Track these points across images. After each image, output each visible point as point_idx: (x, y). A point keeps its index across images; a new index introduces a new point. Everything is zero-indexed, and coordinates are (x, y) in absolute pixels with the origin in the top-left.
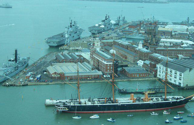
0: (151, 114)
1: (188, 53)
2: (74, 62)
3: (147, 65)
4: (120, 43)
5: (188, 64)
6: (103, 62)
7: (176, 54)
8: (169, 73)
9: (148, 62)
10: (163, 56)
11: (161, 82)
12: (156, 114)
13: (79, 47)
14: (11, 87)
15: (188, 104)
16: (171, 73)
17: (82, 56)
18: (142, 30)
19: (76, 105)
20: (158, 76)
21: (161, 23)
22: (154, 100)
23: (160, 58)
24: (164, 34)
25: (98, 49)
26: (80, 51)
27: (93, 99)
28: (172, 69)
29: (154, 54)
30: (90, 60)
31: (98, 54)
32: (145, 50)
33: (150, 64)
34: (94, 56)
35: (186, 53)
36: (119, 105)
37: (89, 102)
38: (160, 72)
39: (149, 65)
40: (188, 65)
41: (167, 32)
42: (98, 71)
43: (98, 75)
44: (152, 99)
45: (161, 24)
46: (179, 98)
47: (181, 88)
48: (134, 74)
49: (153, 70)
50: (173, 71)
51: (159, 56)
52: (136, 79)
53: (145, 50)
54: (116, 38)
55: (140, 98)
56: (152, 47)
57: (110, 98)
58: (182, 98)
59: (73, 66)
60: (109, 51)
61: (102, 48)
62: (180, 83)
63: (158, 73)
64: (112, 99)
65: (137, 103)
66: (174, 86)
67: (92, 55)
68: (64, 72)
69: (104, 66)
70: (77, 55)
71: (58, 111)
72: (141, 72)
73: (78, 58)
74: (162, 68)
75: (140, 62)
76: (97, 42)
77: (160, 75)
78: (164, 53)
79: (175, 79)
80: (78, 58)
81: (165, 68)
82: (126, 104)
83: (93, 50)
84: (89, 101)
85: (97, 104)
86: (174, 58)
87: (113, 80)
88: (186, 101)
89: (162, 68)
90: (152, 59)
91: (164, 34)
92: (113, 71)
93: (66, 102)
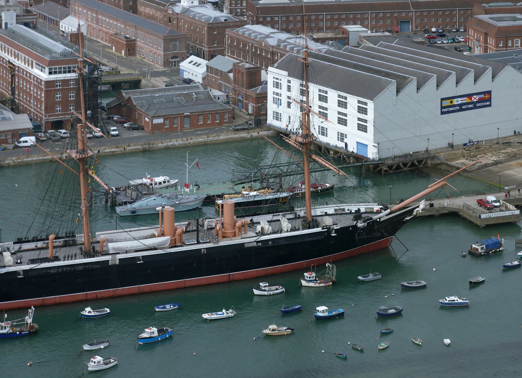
0: (256, 292)
1: (384, 18)
3: (223, 75)
6: (36, 71)
7: (336, 24)
8: (315, 104)
10: (284, 36)
11: (288, 146)
15: (401, 235)
16: (324, 104)
20: (271, 120)
22: (259, 228)
23: (272, 42)
29: (247, 26)
33: (235, 69)
36: (114, 266)
38: (278, 102)
39: (231, 75)
40: (391, 68)
42: (9, 114)
46: (363, 210)
49: (247, 97)
50: (333, 95)
52: (177, 137)
55: (203, 226)
60: (57, 24)
63: (271, 107)
64: (81, 238)
69: (38, 88)
72: (200, 108)
75: (191, 66)
77: (277, 116)
78: (288, 22)
79: (342, 129)
81: (296, 84)
82: (143, 257)
87: (84, 151)
92: (78, 108)
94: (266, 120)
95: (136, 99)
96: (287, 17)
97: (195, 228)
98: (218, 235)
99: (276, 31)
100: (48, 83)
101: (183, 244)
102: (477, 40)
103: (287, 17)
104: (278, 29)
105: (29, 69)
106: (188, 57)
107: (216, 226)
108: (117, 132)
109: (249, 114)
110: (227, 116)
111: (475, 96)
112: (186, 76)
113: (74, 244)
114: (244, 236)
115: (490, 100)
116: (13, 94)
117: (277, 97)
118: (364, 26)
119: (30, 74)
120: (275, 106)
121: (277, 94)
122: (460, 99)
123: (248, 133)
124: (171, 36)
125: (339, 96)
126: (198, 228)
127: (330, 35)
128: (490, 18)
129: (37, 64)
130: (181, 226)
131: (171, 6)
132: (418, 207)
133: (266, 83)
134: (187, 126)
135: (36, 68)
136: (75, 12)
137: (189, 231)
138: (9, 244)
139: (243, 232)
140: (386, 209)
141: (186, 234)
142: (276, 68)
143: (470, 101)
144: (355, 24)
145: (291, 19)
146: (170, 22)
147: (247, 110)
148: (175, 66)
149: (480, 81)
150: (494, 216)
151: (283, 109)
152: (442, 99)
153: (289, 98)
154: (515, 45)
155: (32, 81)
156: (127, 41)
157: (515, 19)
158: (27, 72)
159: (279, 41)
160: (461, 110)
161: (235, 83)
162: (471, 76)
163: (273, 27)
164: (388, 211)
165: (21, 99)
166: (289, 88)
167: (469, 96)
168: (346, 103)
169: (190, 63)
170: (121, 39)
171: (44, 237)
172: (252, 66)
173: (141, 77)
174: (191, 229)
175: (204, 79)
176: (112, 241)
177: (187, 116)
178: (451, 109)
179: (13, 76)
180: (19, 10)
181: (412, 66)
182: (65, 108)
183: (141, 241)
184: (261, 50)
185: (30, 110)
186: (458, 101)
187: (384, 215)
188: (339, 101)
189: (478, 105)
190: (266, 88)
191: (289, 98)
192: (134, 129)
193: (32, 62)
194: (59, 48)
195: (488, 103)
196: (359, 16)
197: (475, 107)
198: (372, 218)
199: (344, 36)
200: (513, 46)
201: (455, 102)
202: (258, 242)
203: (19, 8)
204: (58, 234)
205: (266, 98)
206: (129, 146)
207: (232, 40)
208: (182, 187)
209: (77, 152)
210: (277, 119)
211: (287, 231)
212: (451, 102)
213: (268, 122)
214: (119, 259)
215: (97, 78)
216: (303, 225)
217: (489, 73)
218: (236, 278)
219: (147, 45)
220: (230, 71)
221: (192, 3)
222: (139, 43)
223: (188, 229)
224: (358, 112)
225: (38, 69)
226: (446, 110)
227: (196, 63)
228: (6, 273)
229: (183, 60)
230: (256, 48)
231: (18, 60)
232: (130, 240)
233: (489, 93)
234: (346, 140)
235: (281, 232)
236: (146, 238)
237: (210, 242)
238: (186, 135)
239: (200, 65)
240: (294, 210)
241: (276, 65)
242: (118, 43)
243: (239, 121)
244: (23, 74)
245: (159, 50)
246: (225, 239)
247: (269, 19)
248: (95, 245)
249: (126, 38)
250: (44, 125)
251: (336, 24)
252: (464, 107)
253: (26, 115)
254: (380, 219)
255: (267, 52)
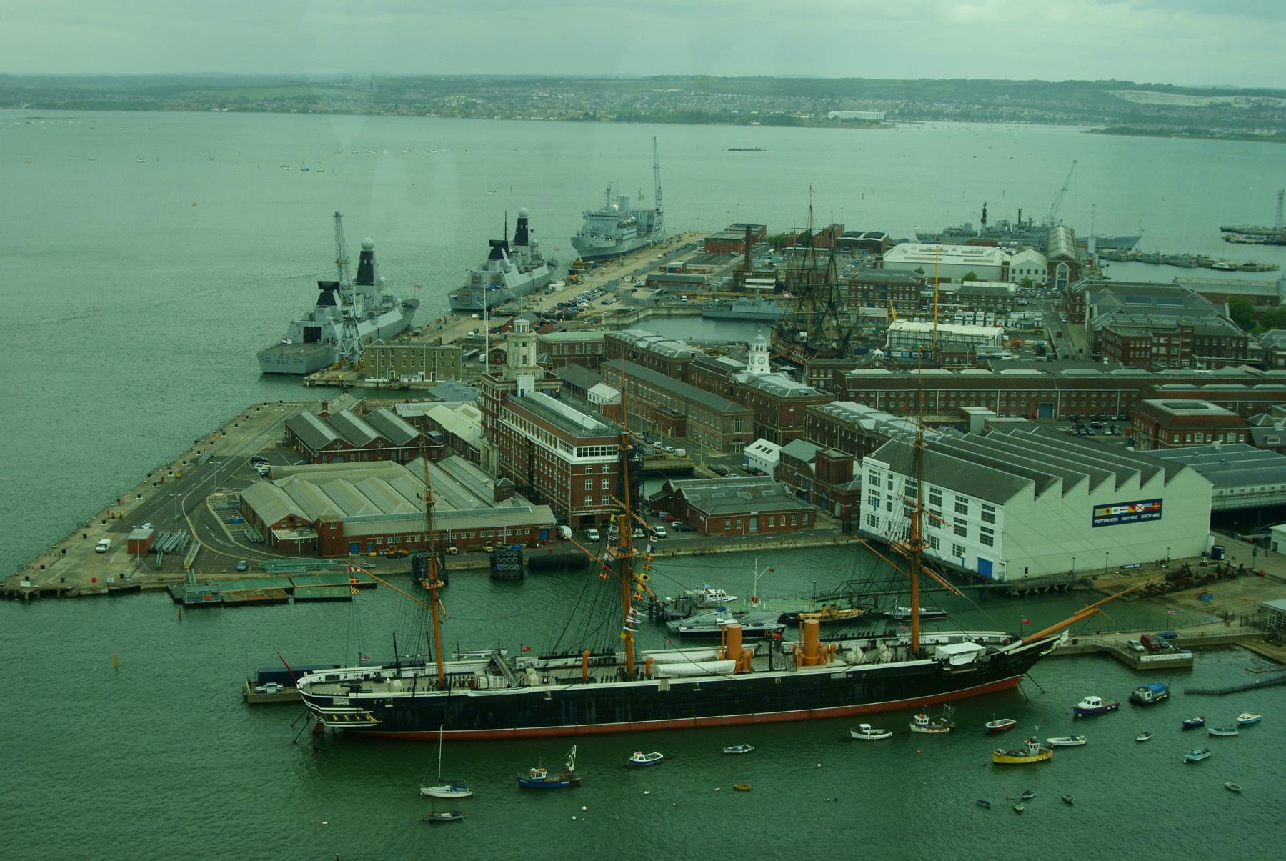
2: (393, 455)
3: (803, 466)
4: (642, 345)
5: (1026, 454)
6: (560, 452)
9: (804, 450)
10: (884, 417)
12: (882, 735)
13: (413, 372)
14: (47, 609)
15: (1033, 671)
17: (435, 425)
18: (757, 275)
19: (420, 694)
20: (864, 526)
21: (857, 234)
22: (851, 656)
23: (868, 424)
24: (884, 295)
25: (527, 384)
26: (423, 394)
27: (513, 660)
28: (939, 488)
29: (837, 403)
30: (481, 444)
31: (531, 410)
32: (783, 383)
33: (819, 458)
34: (506, 422)
35: (1008, 398)
36: (664, 692)
37: (491, 677)
38: (875, 503)
39: (813, 466)
41: (898, 285)
42: (525, 504)
43: (534, 528)
44: (841, 651)
45: (861, 238)
47: (992, 590)
48: (733, 518)
49: (835, 495)
51: (864, 417)
52: (741, 542)
53: (783, 383)
54: (614, 321)
56: (819, 368)
57: (610, 652)
58: (1005, 644)
59: (388, 479)
61: (548, 376)
62: (985, 565)
63: (866, 509)
64: (620, 656)
65: (760, 673)
66: (957, 575)
67: (494, 416)
68: (343, 516)
69: (563, 473)
70: (406, 419)
71: (318, 731)
72: (772, 507)
73: (413, 432)
74: (884, 478)
75: (759, 453)
76: (520, 342)
77: (873, 521)
78: (888, 398)
79: (959, 540)
80: (413, 432)
81: (900, 481)
83: (500, 388)
84: (493, 667)
85: (535, 685)
86: (947, 424)
88: (1028, 659)
89: (884, 478)
90: (826, 431)
91: (884, 295)
93: (367, 677)
94: (858, 525)
95: (688, 492)
96: (888, 394)
97: (767, 652)
98: (795, 661)
99: (874, 410)
100: (578, 468)
101: (753, 671)
102: (1144, 432)
103: (888, 394)
104: (875, 407)
105: (552, 449)
106: (755, 440)
107: (794, 650)
108: (664, 533)
109: (835, 517)
110: (806, 518)
111: (1140, 505)
112: (752, 464)
113: (614, 664)
114: (829, 664)
115: (1159, 510)
116: (531, 480)
117: (874, 496)
118: (990, 409)
119: (553, 455)
120: (871, 508)
121: (874, 492)
122: (1119, 508)
123: (835, 541)
124: (733, 413)
125: (957, 498)
126: (771, 652)
127: (944, 419)
128: (1164, 404)
129: (561, 442)
130: (749, 648)
131: (733, 374)
132: (1059, 639)
133: (860, 477)
134: (753, 529)
135: (561, 447)
136: (607, 378)
137: (760, 656)
138: (534, 660)
139: (829, 660)
140: (1017, 639)
141: (755, 659)
142: (874, 458)
143: (1133, 511)
144: (978, 405)
145: (892, 395)
146: (732, 394)
147: (833, 510)
148: (738, 451)
149: (1148, 485)
150: (1158, 659)
151: (882, 513)
152: (1096, 507)
153: (890, 497)
154: (1196, 441)
155: (556, 464)
156: (674, 418)
157: (1197, 407)
158: (548, 452)
159: (878, 423)
160: (1120, 522)
161: (818, 477)
162: (1136, 479)
163: (869, 406)
164: (1020, 642)
165: (540, 486)
166: (890, 486)
167: (1132, 504)
168: (966, 507)
169: (758, 448)
170: (668, 415)
171: (576, 653)
172: (842, 455)
173: (693, 465)
174: (762, 653)
175: (776, 469)
176: (661, 662)
177: (754, 516)
178: (1107, 520)
179: (531, 458)
180: (541, 372)
181: (1056, 462)
182: (597, 500)
183: (698, 664)
184: (853, 435)
185: (552, 501)
186: (1115, 511)
187: (1013, 648)
188: (956, 504)
189: (1143, 517)
190: (860, 484)
191: (890, 497)
192: (683, 530)
193: (556, 439)
194: (590, 423)
195: (1157, 515)
196: (983, 395)
197: (1139, 520)
198: (998, 651)
199: (963, 420)
200: (1192, 442)
201: (1113, 511)
202: (847, 673)
203: (538, 370)
204: (593, 650)
205: (859, 497)
206: (679, 551)
207: (815, 419)
208: (748, 601)
209: (619, 550)
210: (873, 524)
211: (887, 662)
212: (1108, 511)
213: (861, 528)
214: (671, 685)
215: (638, 463)
216: (908, 655)
217: (1161, 475)
218: (819, 715)
219: (701, 423)
220: (811, 461)
221: (762, 370)
222: (692, 420)
223: (758, 653)
224: (982, 519)
225: (564, 449)
226: (1100, 521)
227: (766, 449)
228: (531, 693)
229: (748, 445)
230: (846, 432)
231: (538, 437)
232: (684, 662)
233: (1159, 501)
234: (963, 555)
235: (878, 662)
236: (703, 660)
237: (786, 670)
238: (751, 539)
239: (770, 451)
240: (896, 636)
241: (874, 454)
242: (663, 419)
243: (819, 526)
244: (544, 455)
245: (717, 430)
246: (806, 667)
247: (863, 395)
248: (640, 666)
249: (673, 413)
250: (570, 521)
251: (952, 404)
252: (1123, 519)
253: (548, 506)
254: (1008, 651)
255: (861, 437)
